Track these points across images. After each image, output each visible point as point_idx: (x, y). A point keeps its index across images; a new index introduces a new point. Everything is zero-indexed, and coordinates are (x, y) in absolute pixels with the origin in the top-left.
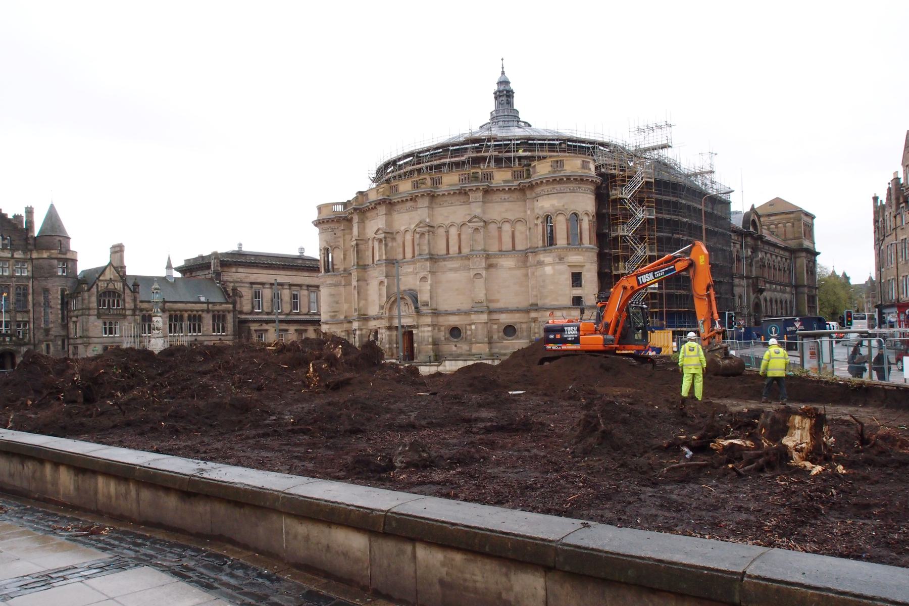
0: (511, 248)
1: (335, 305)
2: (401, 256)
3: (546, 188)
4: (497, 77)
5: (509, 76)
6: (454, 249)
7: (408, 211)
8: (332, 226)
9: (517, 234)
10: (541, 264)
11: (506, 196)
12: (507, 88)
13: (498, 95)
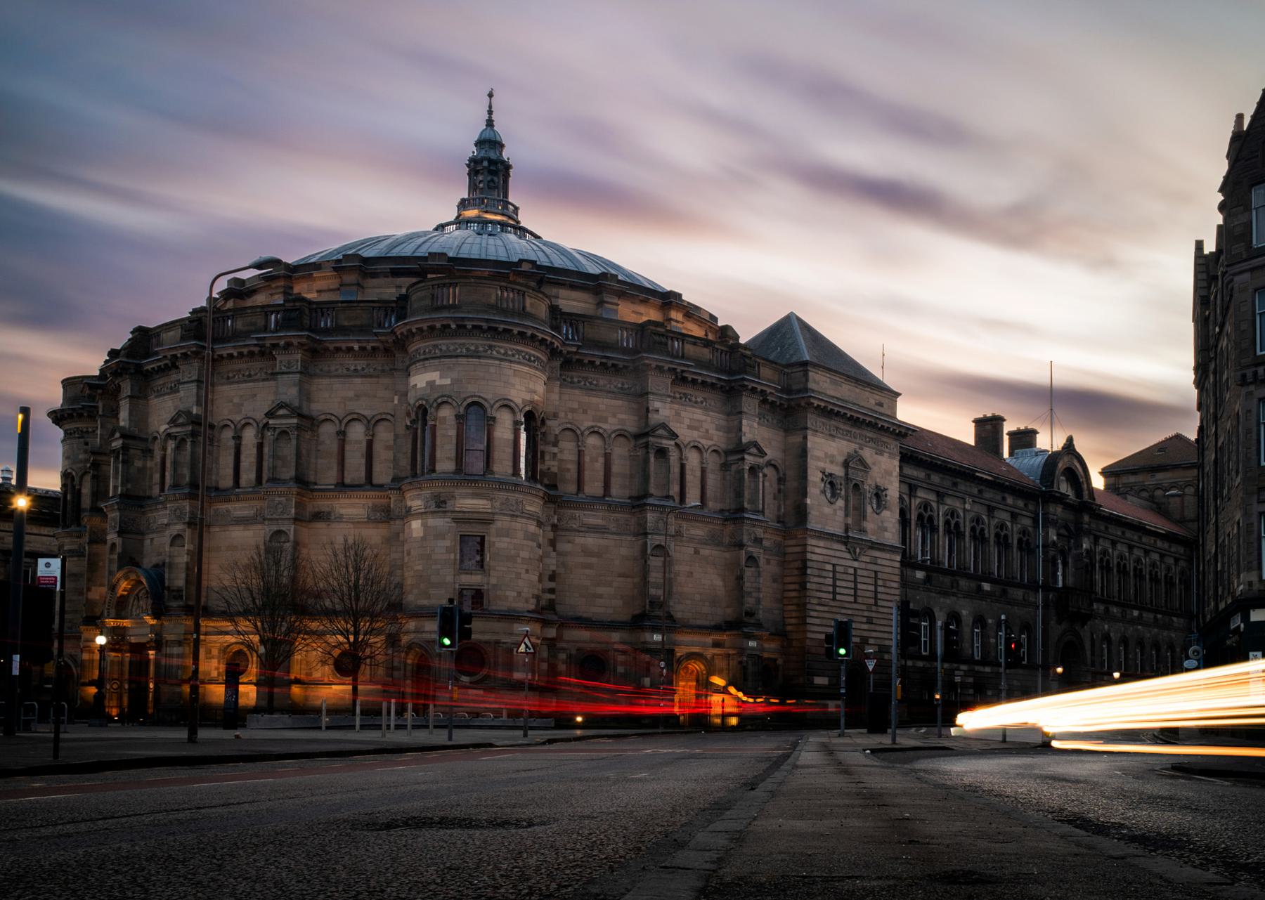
0: (363, 481)
4: (476, 129)
6: (248, 476)
9: (378, 447)
11: (360, 364)
13: (475, 167)
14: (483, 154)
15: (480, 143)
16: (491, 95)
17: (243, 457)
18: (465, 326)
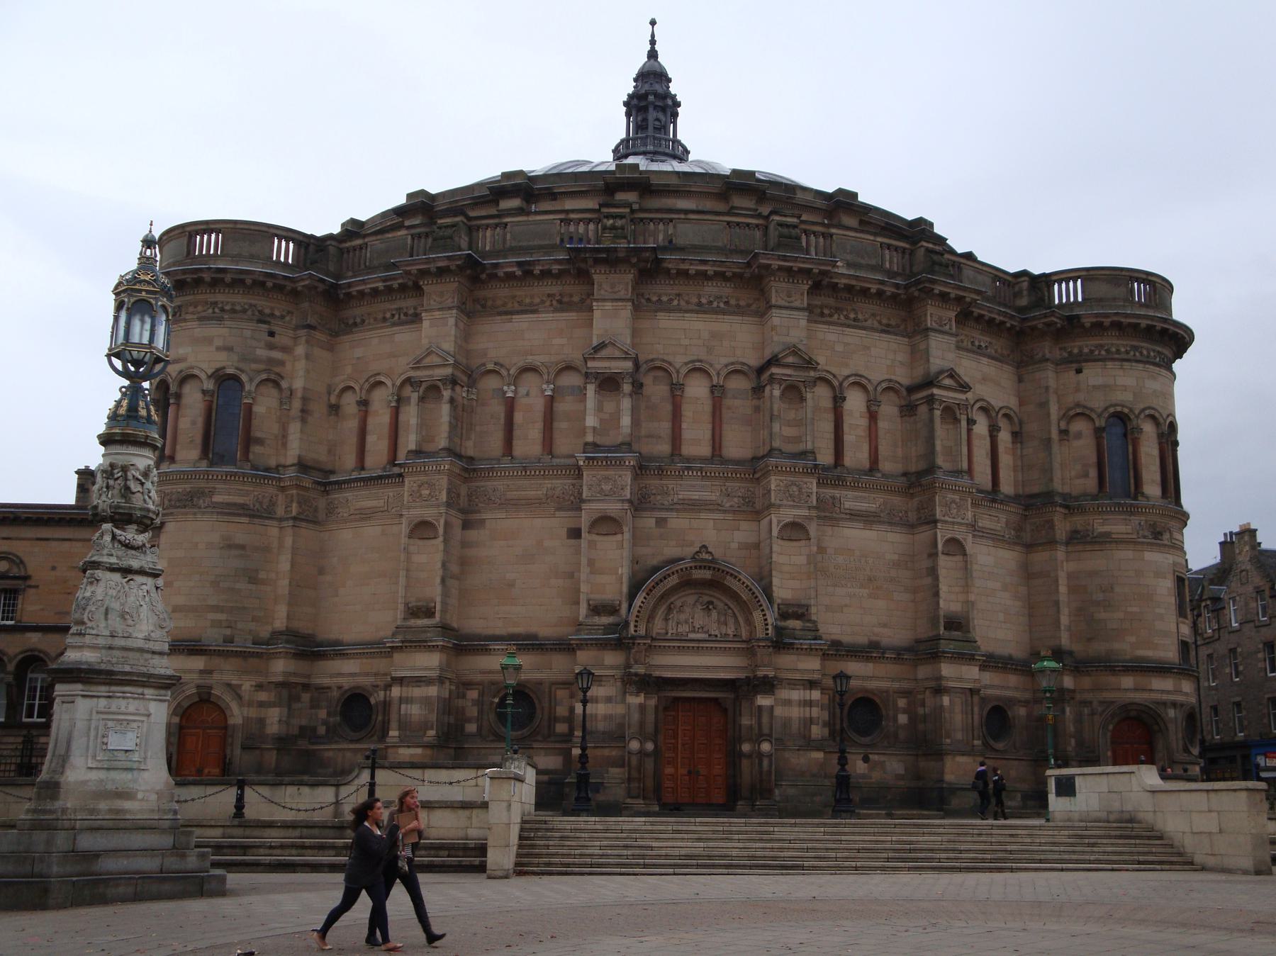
1: (242, 585)
2: (664, 448)
3: (1113, 342)
6: (856, 455)
7: (701, 309)
8: (276, 305)
12: (658, 88)
14: (647, 87)
15: (642, 77)
17: (846, 428)
18: (496, 275)
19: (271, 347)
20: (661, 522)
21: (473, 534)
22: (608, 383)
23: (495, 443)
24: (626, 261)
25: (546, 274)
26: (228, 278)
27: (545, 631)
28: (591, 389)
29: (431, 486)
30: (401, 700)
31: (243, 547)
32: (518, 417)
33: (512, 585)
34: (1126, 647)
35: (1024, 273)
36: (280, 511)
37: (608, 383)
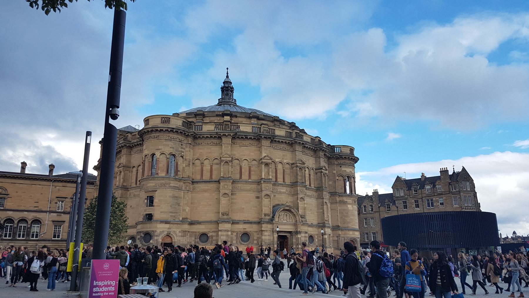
3: (347, 161)
5: (231, 78)
7: (280, 149)
10: (345, 203)
16: (227, 69)
19: (182, 148)
20: (275, 196)
21: (234, 197)
22: (267, 164)
23: (238, 176)
24: (270, 138)
25: (251, 138)
26: (174, 131)
27: (251, 220)
28: (263, 166)
29: (227, 185)
30: (221, 235)
31: (177, 197)
32: (243, 170)
33: (243, 209)
34: (351, 225)
35: (329, 145)
36: (183, 188)
37: (267, 164)
